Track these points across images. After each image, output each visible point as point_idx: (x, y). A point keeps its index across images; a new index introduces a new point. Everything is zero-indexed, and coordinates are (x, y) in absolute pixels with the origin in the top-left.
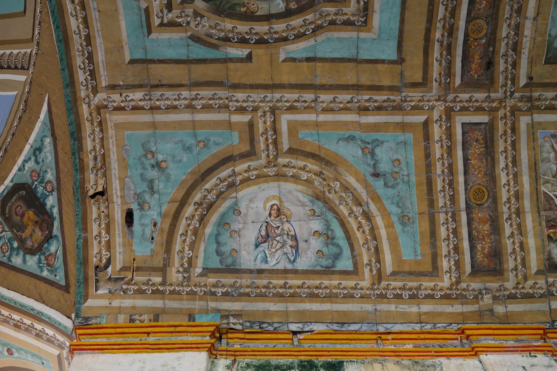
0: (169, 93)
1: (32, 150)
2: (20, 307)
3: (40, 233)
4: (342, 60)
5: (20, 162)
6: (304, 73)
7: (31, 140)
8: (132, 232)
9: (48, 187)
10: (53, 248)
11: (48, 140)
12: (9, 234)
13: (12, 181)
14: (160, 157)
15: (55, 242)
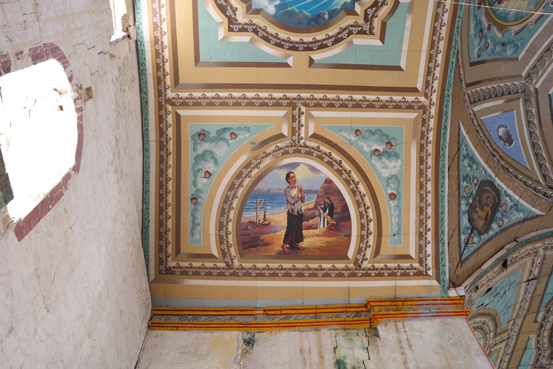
0: (533, 288)
1: (516, 202)
2: (440, 219)
3: (481, 225)
4: (521, 360)
5: (509, 192)
6: (521, 346)
7: (521, 201)
8: (484, 295)
9: (500, 222)
10: (476, 239)
11: (521, 215)
12: (474, 192)
13: (499, 185)
14: (507, 293)
15: (478, 239)
